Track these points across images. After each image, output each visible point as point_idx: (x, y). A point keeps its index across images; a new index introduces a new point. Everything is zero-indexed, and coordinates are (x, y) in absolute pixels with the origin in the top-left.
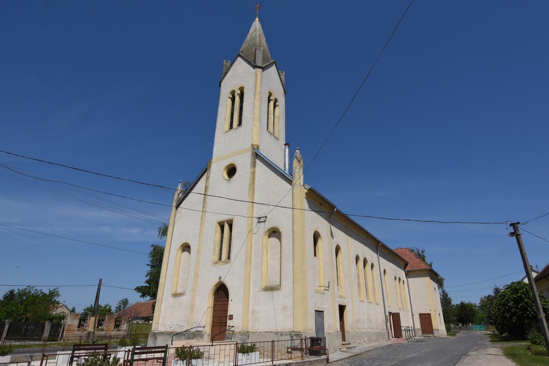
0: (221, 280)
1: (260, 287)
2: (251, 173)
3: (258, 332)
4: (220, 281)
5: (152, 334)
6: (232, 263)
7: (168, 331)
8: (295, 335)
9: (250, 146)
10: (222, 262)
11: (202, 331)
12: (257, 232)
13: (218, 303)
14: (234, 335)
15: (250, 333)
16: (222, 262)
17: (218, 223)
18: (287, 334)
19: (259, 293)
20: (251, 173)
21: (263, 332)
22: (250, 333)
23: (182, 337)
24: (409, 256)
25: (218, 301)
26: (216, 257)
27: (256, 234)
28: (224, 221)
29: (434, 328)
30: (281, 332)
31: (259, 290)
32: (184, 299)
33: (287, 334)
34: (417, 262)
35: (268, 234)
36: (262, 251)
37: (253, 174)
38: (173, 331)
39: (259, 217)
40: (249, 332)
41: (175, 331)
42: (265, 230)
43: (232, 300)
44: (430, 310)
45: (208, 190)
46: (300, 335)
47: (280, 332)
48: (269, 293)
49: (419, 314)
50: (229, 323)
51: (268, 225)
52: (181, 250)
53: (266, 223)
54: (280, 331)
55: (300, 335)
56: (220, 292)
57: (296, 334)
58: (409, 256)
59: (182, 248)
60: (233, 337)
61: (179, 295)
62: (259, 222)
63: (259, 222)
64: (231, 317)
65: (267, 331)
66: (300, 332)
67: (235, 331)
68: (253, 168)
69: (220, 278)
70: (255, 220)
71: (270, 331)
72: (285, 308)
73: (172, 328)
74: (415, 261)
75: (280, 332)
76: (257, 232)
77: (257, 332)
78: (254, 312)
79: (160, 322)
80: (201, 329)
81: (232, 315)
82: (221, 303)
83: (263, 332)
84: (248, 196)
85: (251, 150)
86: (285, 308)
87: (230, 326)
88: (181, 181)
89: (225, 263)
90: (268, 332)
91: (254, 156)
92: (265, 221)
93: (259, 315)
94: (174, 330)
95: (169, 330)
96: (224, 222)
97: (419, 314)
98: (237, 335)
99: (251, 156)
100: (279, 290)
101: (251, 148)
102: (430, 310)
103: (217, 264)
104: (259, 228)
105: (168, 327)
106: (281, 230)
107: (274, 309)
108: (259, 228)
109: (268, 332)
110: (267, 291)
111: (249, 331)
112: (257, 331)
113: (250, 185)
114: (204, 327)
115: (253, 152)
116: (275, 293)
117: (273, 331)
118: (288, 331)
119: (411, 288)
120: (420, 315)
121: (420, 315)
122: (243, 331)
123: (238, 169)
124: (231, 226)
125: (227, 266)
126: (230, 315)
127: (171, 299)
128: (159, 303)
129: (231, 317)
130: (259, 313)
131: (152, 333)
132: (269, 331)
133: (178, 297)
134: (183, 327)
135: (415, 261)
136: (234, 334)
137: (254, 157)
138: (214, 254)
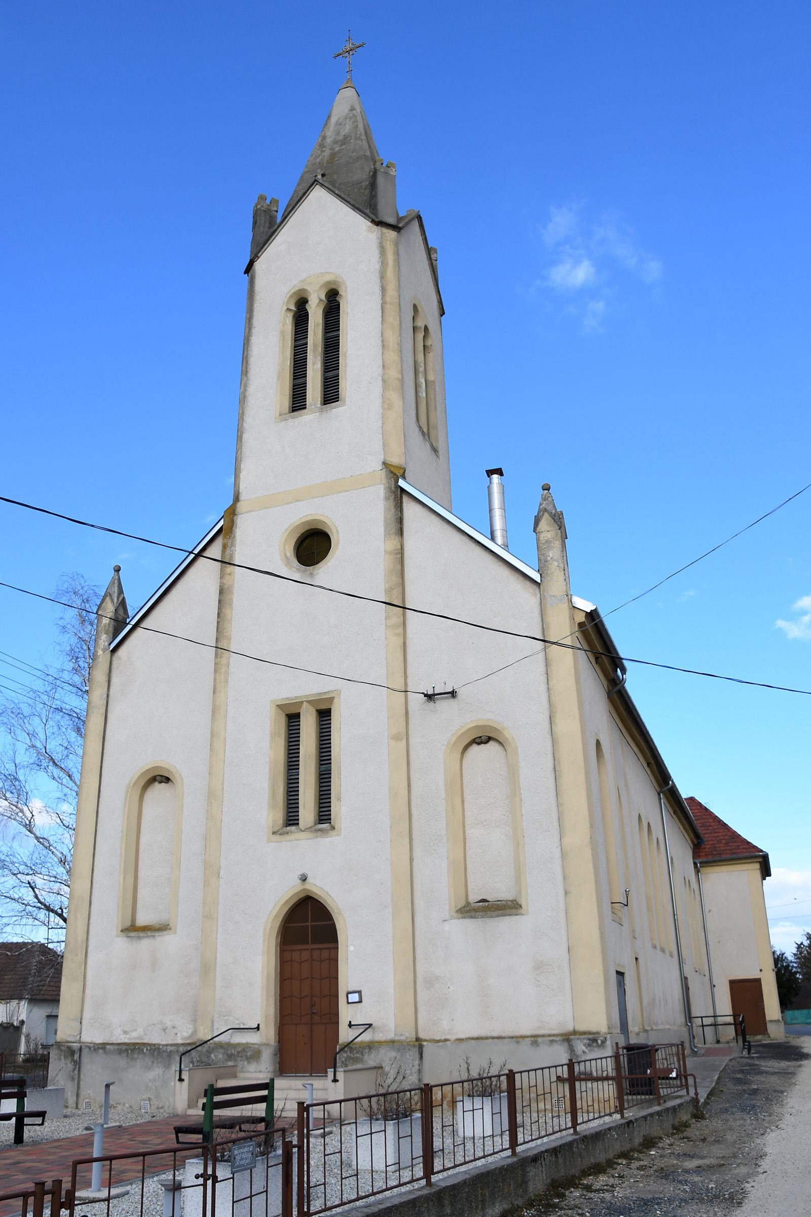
2: (390, 553)
9: (380, 466)
18: (552, 1041)
20: (390, 553)
22: (425, 1043)
24: (702, 821)
26: (279, 815)
28: (302, 702)
29: (768, 1018)
32: (167, 943)
34: (727, 837)
37: (400, 555)
39: (431, 692)
44: (761, 970)
45: (231, 600)
49: (730, 981)
54: (529, 1033)
55: (599, 1042)
58: (702, 821)
69: (304, 879)
74: (720, 834)
85: (384, 482)
86: (539, 967)
87: (352, 1023)
94: (141, 1038)
95: (124, 1039)
97: (730, 981)
99: (387, 499)
102: (761, 970)
112: (448, 1037)
116: (504, 924)
119: (710, 911)
120: (733, 983)
121: (733, 983)
124: (324, 715)
125: (326, 842)
127: (121, 944)
128: (77, 955)
133: (147, 937)
135: (720, 834)
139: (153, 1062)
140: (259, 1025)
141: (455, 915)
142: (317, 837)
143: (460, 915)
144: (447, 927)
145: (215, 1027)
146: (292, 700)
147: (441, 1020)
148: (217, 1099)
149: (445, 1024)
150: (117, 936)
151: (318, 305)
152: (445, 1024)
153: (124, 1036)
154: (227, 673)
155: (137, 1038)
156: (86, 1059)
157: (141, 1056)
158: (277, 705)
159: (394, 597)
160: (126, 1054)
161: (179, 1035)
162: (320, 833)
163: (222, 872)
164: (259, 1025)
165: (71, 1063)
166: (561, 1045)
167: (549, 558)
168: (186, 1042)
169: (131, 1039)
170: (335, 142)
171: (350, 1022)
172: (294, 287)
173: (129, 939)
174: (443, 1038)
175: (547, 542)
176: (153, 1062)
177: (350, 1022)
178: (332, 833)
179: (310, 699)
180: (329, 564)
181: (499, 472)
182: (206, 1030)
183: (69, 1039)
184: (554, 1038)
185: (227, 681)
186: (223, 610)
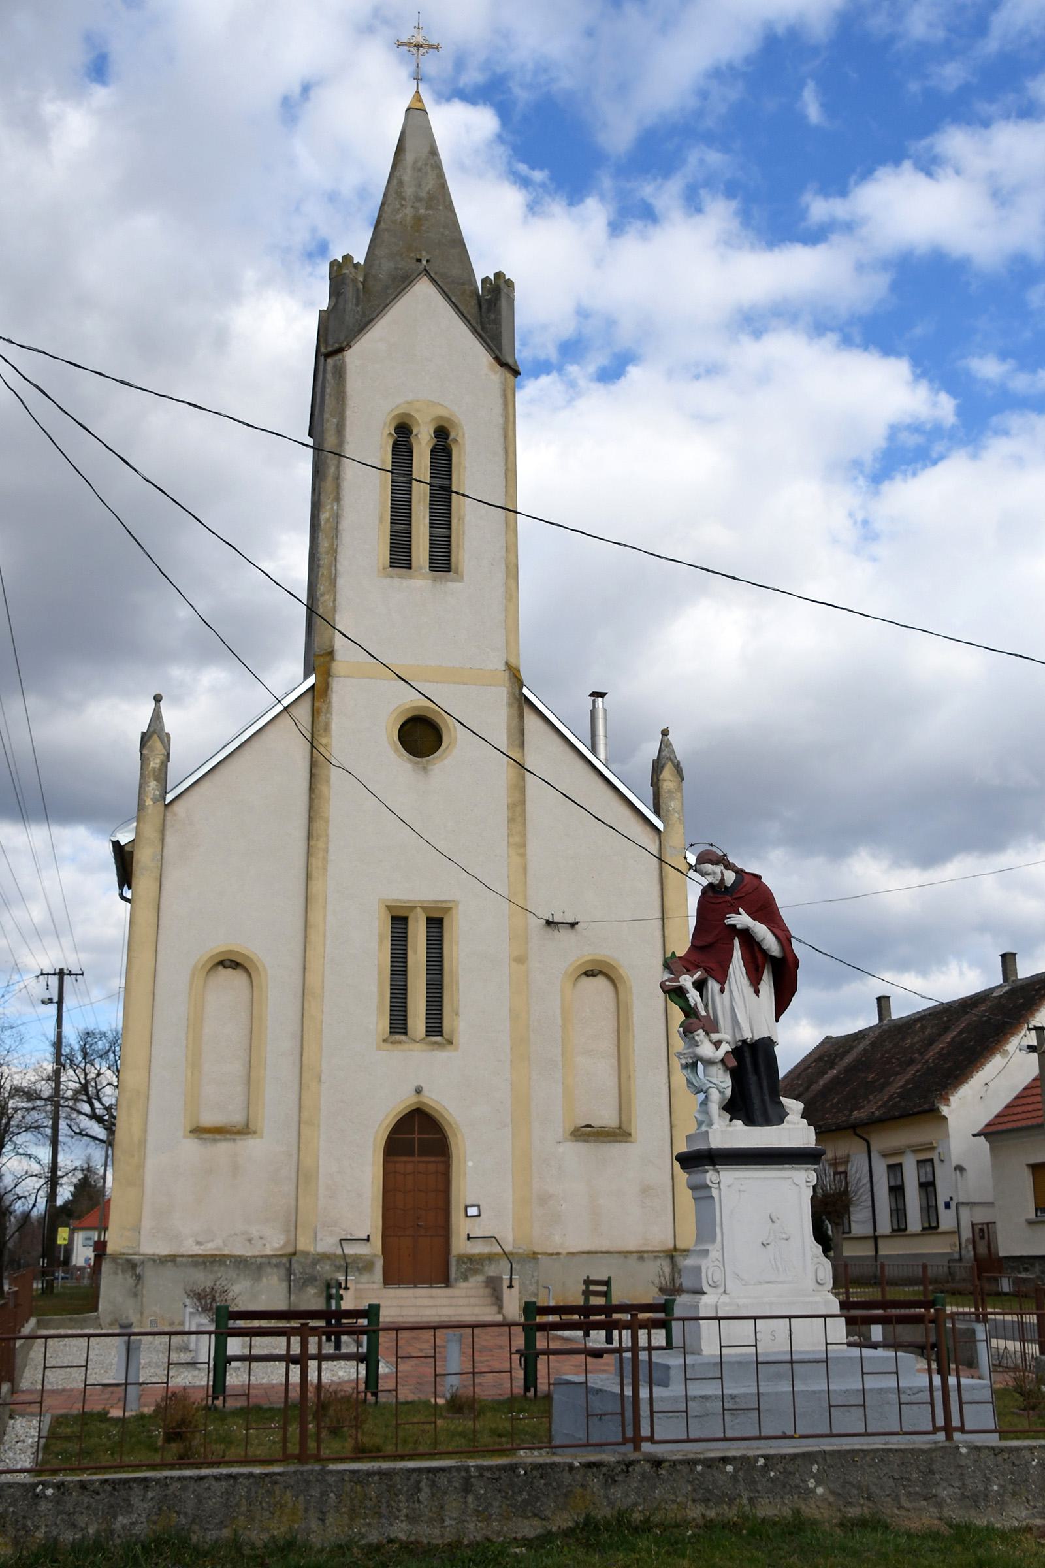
18: (656, 1257)
22: (539, 1256)
23: (269, 1270)
28: (415, 907)
32: (251, 1147)
54: (634, 1250)
69: (419, 1091)
78: (544, 1199)
79: (147, 1224)
100: (626, 1142)
103: (400, 1047)
112: (560, 1251)
113: (511, 807)
116: (614, 1150)
124: (436, 924)
127: (192, 1148)
133: (226, 1140)
139: (238, 1275)
140: (368, 1236)
141: (569, 1137)
142: (433, 1050)
143: (574, 1138)
145: (318, 1239)
146: (404, 902)
148: (592, 1288)
149: (557, 1239)
150: (185, 1137)
151: (427, 444)
152: (557, 1239)
153: (197, 1247)
154: (325, 859)
156: (149, 1274)
158: (387, 906)
160: (203, 1267)
161: (268, 1246)
162: (436, 1046)
163: (323, 1078)
164: (368, 1236)
165: (132, 1277)
167: (670, 809)
170: (418, 199)
171: (468, 1235)
172: (397, 406)
173: (200, 1142)
174: (555, 1251)
175: (670, 791)
176: (238, 1275)
177: (468, 1235)
178: (449, 1047)
179: (425, 905)
180: (446, 762)
182: (308, 1241)
183: (125, 1251)
184: (659, 1254)
185: (325, 869)
186: (319, 786)
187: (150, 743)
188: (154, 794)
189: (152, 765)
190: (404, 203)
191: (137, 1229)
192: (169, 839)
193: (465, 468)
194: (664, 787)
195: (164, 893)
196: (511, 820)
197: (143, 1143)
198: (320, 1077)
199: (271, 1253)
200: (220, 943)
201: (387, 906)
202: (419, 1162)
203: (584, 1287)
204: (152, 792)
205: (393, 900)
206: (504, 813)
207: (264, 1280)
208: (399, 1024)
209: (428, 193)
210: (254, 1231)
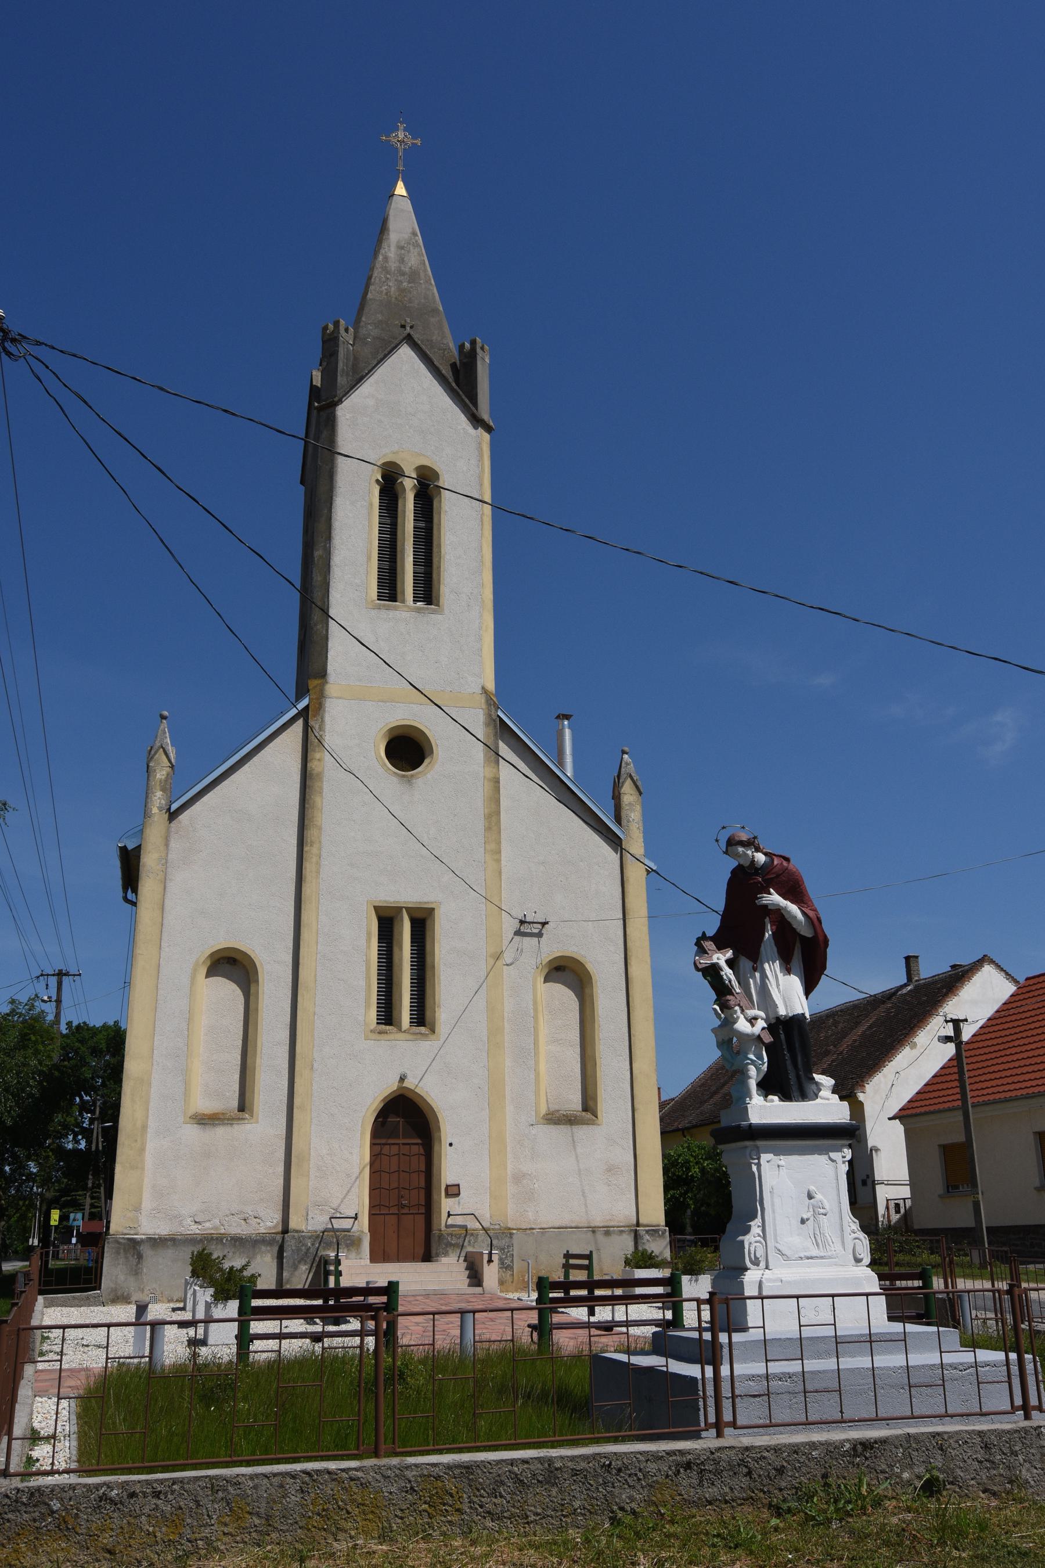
0: (409, 1083)
1: (533, 1113)
2: (489, 780)
3: (538, 1227)
4: (400, 1088)
5: (118, 1243)
6: (442, 1041)
7: (189, 1232)
8: (647, 1232)
10: (405, 1032)
11: (348, 1231)
12: (516, 959)
13: (386, 1150)
14: (472, 1238)
15: (514, 1231)
16: (405, 1032)
17: (377, 909)
18: (621, 1232)
19: (531, 1127)
20: (489, 780)
21: (550, 1228)
22: (514, 1231)
23: (263, 1248)
25: (389, 1144)
27: (511, 964)
28: (401, 908)
30: (603, 1227)
31: (533, 1120)
33: (621, 1232)
35: (546, 971)
36: (536, 1018)
38: (213, 1232)
40: (510, 1229)
41: (223, 1231)
42: (539, 959)
43: (451, 1145)
45: (321, 788)
46: (660, 1233)
47: (600, 1227)
48: (564, 1130)
50: (447, 1204)
51: (551, 948)
52: (203, 971)
53: (543, 940)
54: (601, 1225)
55: (660, 1233)
56: (392, 1119)
57: (649, 1230)
59: (209, 963)
60: (469, 1242)
61: (228, 1119)
62: (518, 933)
63: (518, 933)
64: (453, 1191)
65: (564, 1225)
66: (658, 1226)
67: (469, 1227)
68: (493, 764)
69: (402, 1079)
70: (510, 926)
71: (573, 1225)
72: (611, 1169)
73: (208, 1225)
75: (600, 1227)
76: (516, 959)
77: (533, 1229)
78: (519, 1178)
79: (147, 1204)
80: (346, 1224)
81: (458, 1185)
82: (395, 1149)
83: (550, 1228)
84: (482, 850)
86: (611, 1169)
88: (166, 713)
89: (415, 1037)
90: (566, 1228)
91: (495, 726)
92: (540, 935)
93: (536, 1186)
94: (215, 1228)
95: (195, 1229)
96: (399, 910)
98: (480, 1239)
101: (482, 700)
104: (522, 951)
105: (189, 1221)
106: (590, 967)
107: (579, 1170)
108: (520, 951)
109: (566, 1228)
110: (559, 1124)
111: (510, 1225)
112: (533, 1226)
114: (356, 1218)
115: (490, 715)
116: (581, 1132)
117: (580, 1225)
118: (621, 1224)
122: (497, 1227)
123: (440, 753)
125: (427, 1046)
126: (449, 1183)
127: (192, 1133)
129: (451, 1191)
130: (537, 1180)
131: (121, 1241)
132: (568, 1225)
134: (257, 1220)
136: (472, 1234)
137: (496, 732)
138: (368, 1006)
141: (542, 1121)
143: (545, 1122)
144: (534, 1131)
145: (310, 1217)
146: (391, 903)
147: (527, 1211)
148: (572, 1261)
150: (185, 1123)
151: (411, 489)
152: (531, 1215)
153: (196, 1226)
154: (318, 864)
155: (212, 1229)
156: (146, 1251)
157: (219, 1246)
158: (374, 907)
159: (493, 824)
162: (419, 1036)
163: (315, 1065)
164: (356, 1214)
165: (133, 1256)
166: (628, 1234)
167: (631, 819)
168: (271, 1232)
169: (205, 1230)
171: (449, 1212)
174: (529, 1227)
175: (630, 804)
177: (449, 1212)
178: (432, 1037)
181: (567, 717)
182: (300, 1220)
185: (318, 872)
187: (157, 756)
188: (160, 803)
189: (158, 776)
190: (388, 276)
191: (138, 1209)
192: (173, 844)
193: (446, 512)
194: (625, 800)
195: (168, 895)
196: (488, 829)
197: (145, 1127)
198: (313, 1066)
199: (265, 1231)
200: (221, 941)
201: (374, 907)
202: (403, 1144)
203: (564, 1261)
204: (159, 801)
205: (380, 901)
206: (480, 825)
207: (259, 1257)
208: (387, 1015)
209: (411, 268)
210: (249, 1210)
